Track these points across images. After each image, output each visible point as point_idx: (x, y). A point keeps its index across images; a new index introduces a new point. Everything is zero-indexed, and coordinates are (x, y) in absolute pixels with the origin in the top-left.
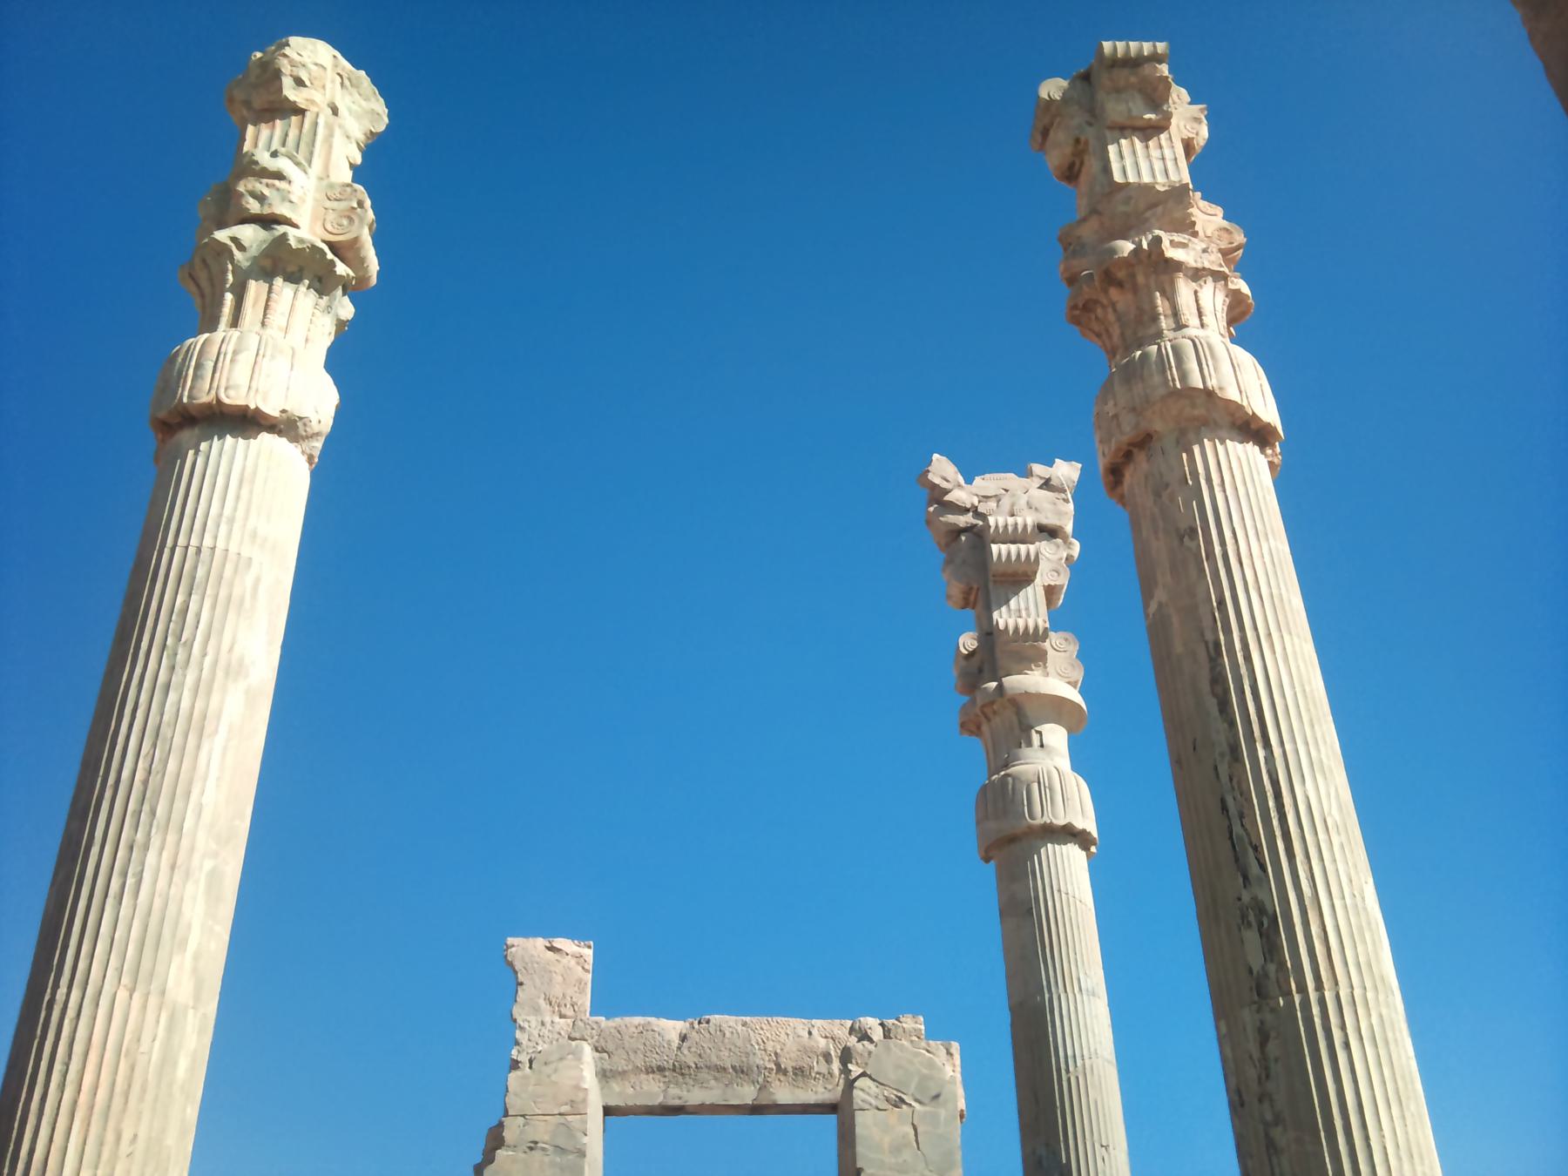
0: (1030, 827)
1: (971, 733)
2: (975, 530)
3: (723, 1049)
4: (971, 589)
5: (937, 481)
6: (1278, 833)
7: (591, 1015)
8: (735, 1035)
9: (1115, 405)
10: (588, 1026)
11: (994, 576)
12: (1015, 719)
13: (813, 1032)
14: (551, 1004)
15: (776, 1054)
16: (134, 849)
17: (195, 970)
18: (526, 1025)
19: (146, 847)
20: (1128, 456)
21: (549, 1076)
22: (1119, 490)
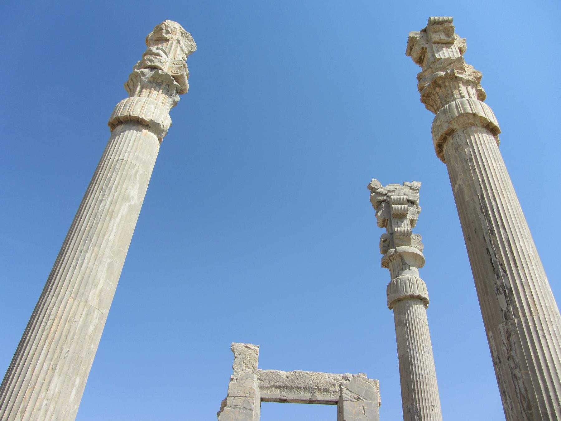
0: (406, 296)
1: (385, 267)
2: (386, 201)
3: (300, 381)
4: (385, 220)
5: (374, 186)
6: (510, 259)
7: (258, 368)
8: (304, 377)
9: (440, 122)
10: (257, 372)
11: (393, 215)
12: (400, 261)
13: (330, 377)
14: (245, 364)
15: (318, 384)
16: (82, 252)
17: (100, 296)
18: (237, 370)
19: (87, 251)
20: (445, 139)
21: (243, 384)
22: (441, 154)
